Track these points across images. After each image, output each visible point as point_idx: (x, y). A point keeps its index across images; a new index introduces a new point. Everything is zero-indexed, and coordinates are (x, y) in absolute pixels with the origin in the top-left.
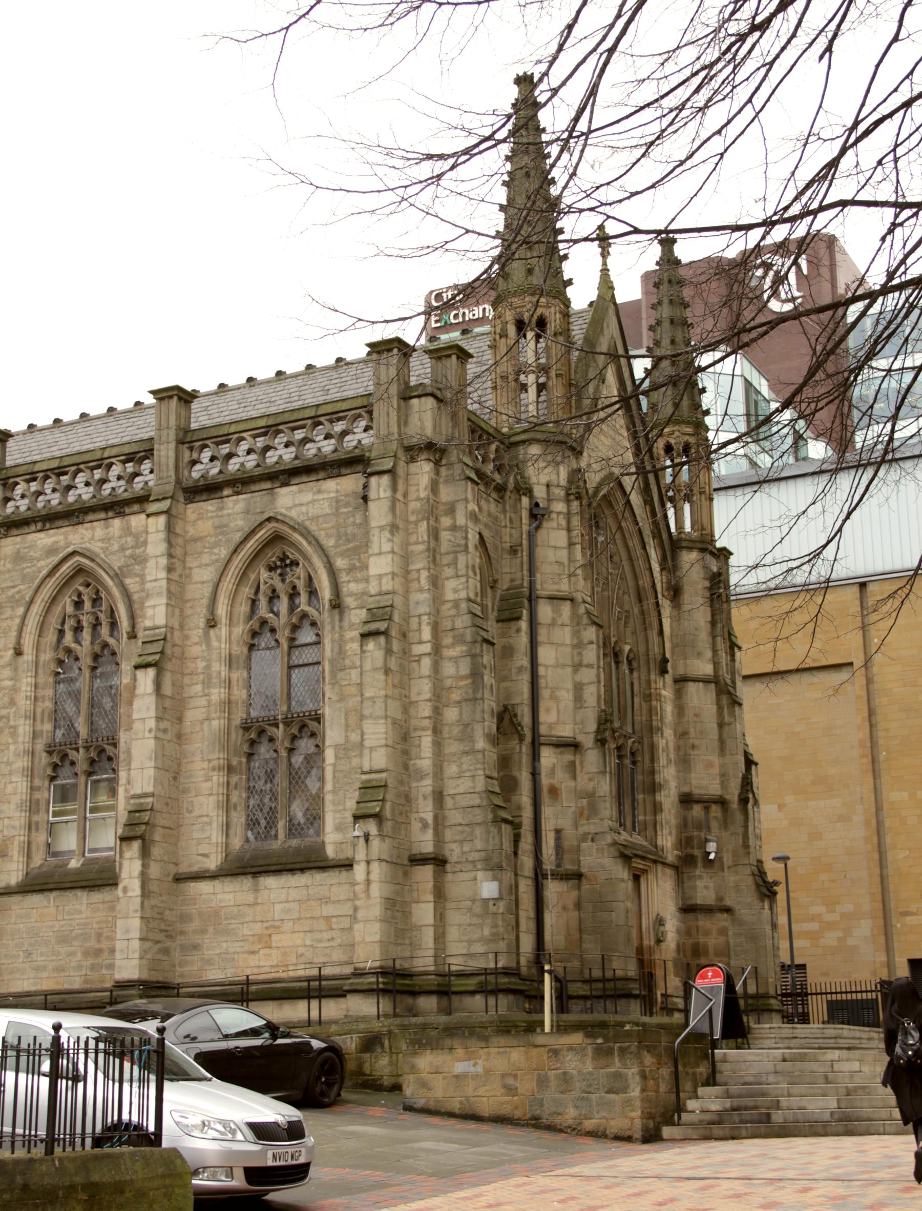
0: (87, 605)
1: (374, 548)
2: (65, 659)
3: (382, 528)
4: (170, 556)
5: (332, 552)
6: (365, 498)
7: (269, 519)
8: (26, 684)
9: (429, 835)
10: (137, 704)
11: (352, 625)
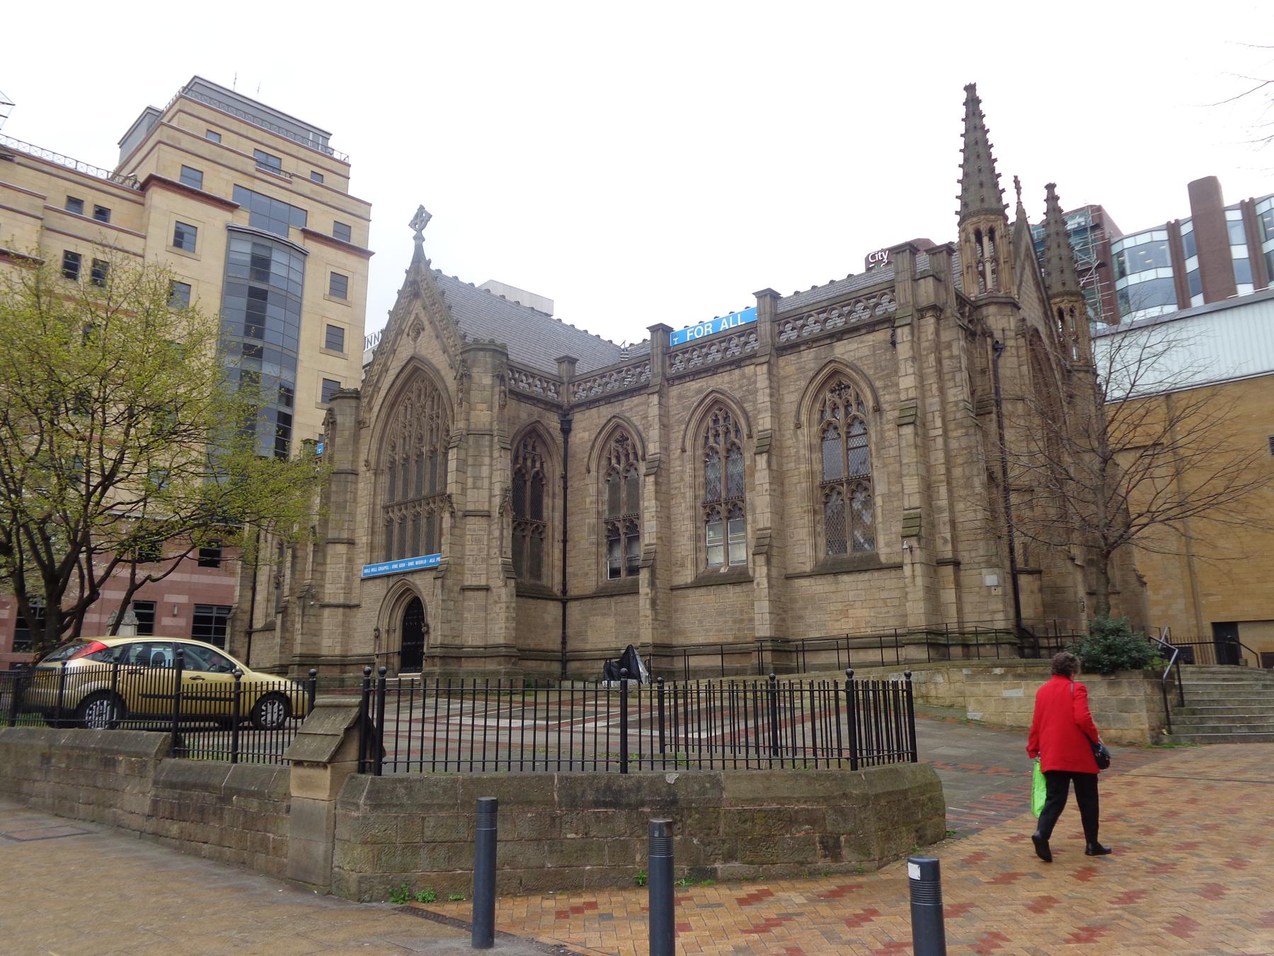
0: (721, 421)
1: (902, 372)
2: (710, 452)
3: (906, 360)
4: (771, 388)
5: (872, 378)
6: (894, 344)
7: (830, 362)
8: (688, 468)
9: (949, 547)
10: (757, 475)
11: (888, 422)
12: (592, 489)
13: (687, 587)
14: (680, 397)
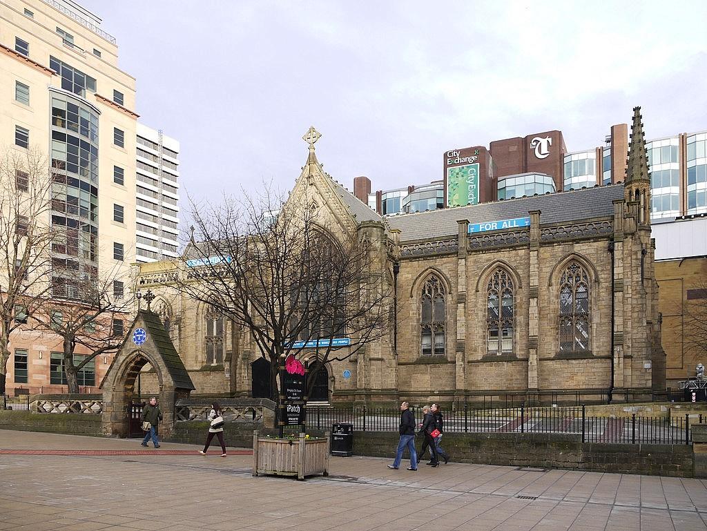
8: (480, 300)
12: (414, 307)
13: (478, 361)
14: (475, 262)
